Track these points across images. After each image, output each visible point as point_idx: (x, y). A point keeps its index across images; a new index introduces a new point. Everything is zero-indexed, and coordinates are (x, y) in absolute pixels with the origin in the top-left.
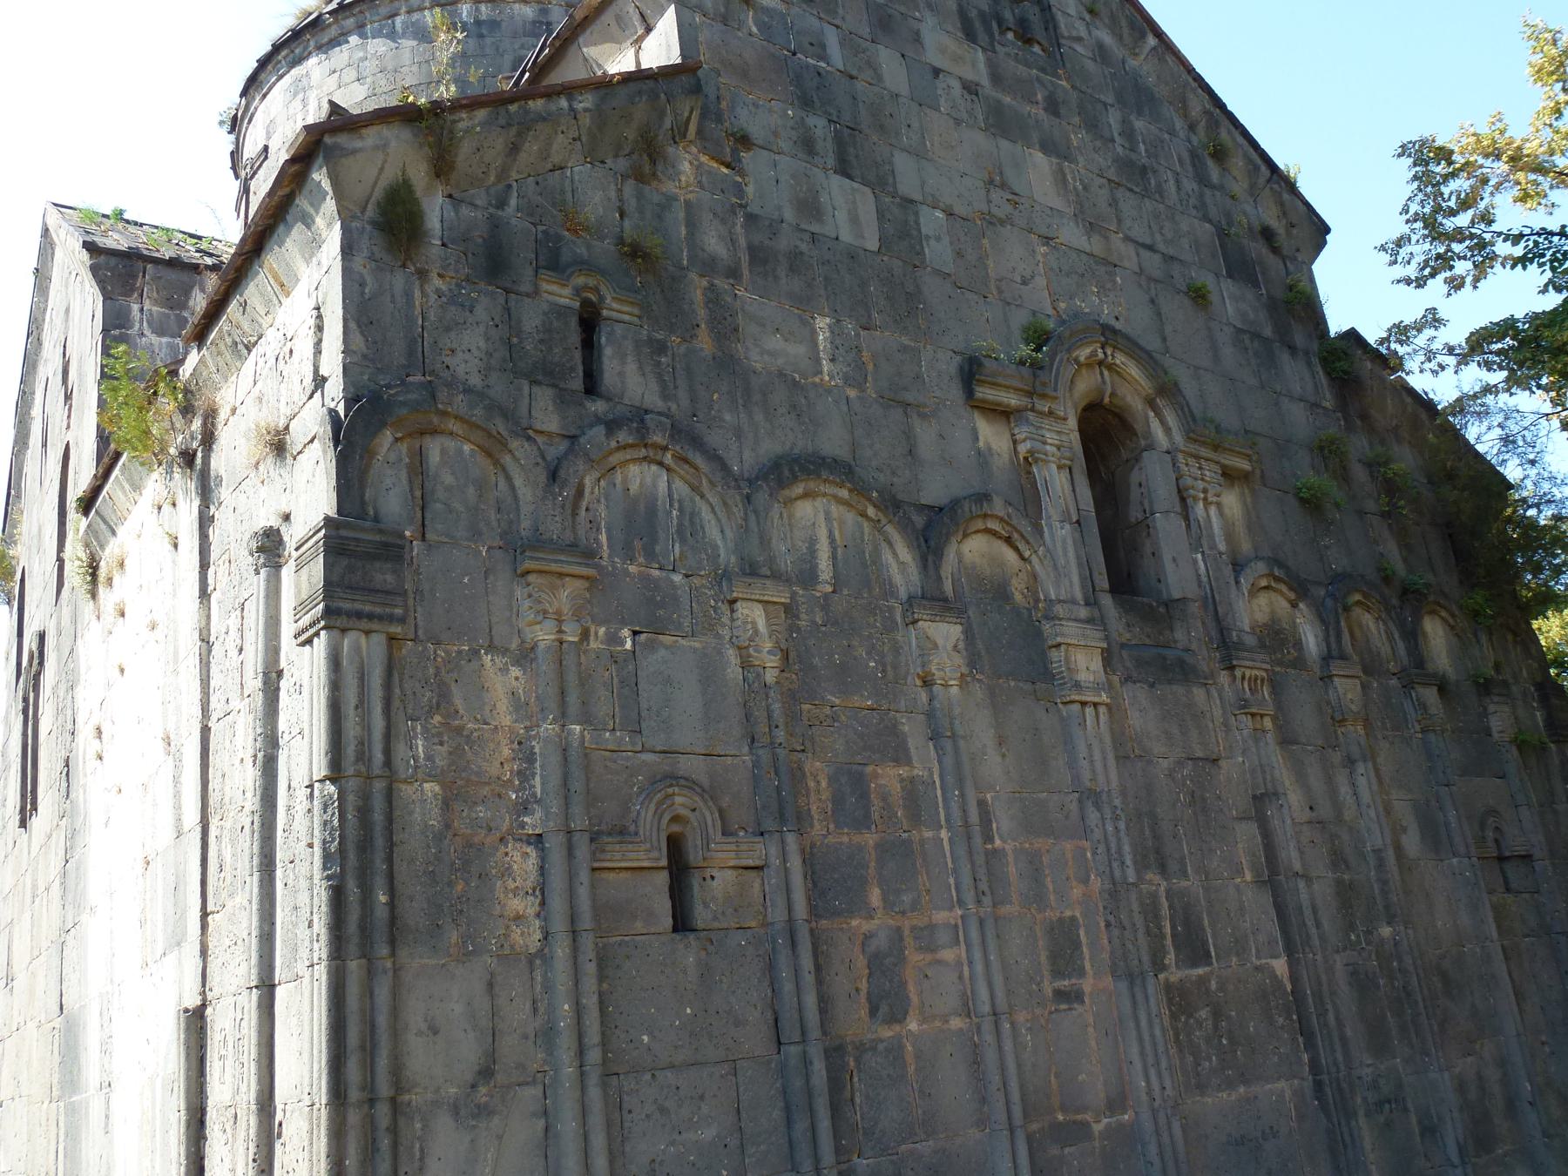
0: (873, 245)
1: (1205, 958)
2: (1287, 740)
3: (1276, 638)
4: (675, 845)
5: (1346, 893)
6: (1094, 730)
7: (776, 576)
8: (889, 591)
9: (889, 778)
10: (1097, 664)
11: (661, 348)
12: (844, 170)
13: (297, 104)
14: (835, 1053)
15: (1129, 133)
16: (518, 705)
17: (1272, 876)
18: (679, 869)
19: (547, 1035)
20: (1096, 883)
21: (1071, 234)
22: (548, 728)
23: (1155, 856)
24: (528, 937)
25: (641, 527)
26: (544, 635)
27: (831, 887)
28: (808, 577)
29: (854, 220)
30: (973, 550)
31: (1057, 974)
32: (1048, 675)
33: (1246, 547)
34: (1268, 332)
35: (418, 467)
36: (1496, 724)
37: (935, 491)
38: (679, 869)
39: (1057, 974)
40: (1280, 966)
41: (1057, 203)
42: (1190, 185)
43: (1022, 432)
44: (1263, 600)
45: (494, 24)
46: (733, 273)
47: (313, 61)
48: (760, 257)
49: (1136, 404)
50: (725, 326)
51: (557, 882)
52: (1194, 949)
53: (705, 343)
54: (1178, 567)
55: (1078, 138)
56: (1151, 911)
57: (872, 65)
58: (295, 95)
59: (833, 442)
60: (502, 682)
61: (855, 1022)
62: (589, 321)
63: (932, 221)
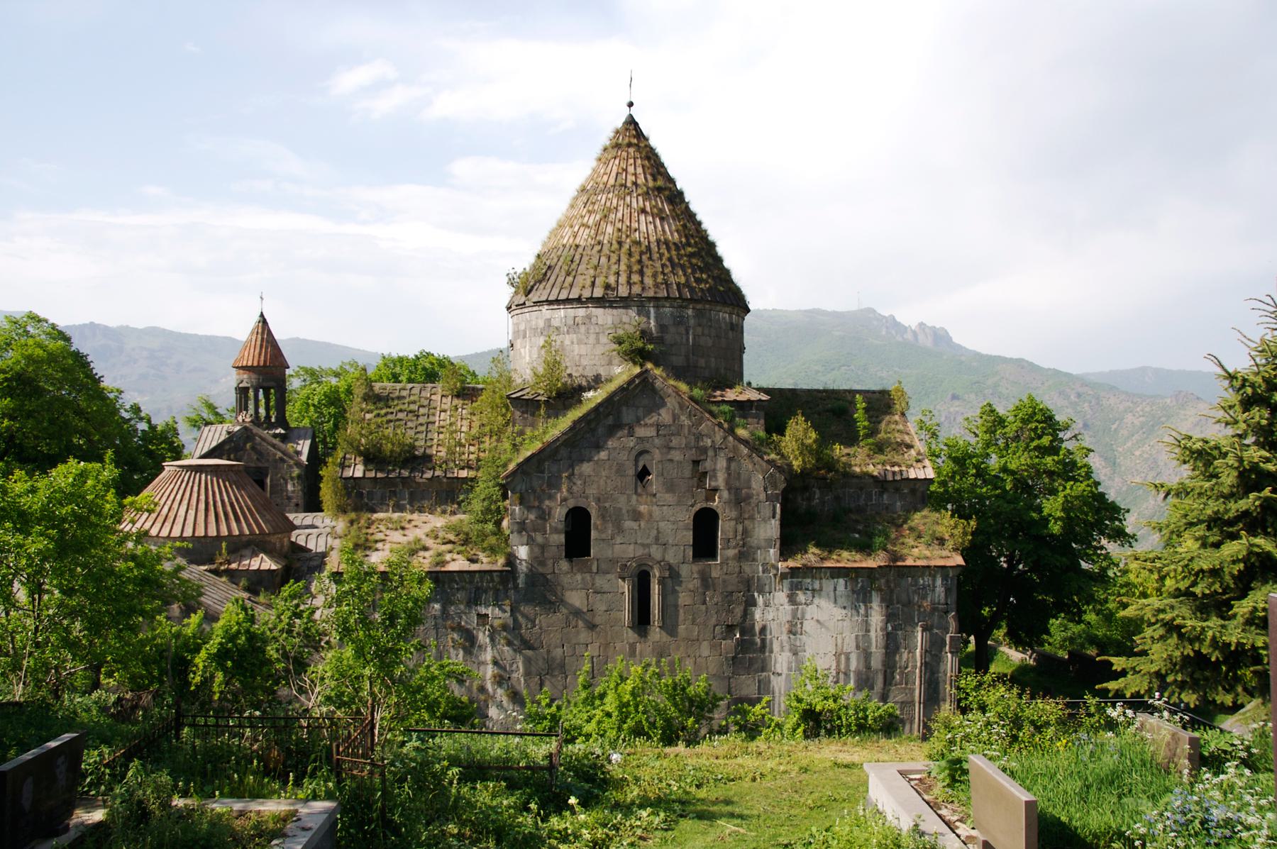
13: (682, 330)
47: (690, 312)
58: (680, 323)
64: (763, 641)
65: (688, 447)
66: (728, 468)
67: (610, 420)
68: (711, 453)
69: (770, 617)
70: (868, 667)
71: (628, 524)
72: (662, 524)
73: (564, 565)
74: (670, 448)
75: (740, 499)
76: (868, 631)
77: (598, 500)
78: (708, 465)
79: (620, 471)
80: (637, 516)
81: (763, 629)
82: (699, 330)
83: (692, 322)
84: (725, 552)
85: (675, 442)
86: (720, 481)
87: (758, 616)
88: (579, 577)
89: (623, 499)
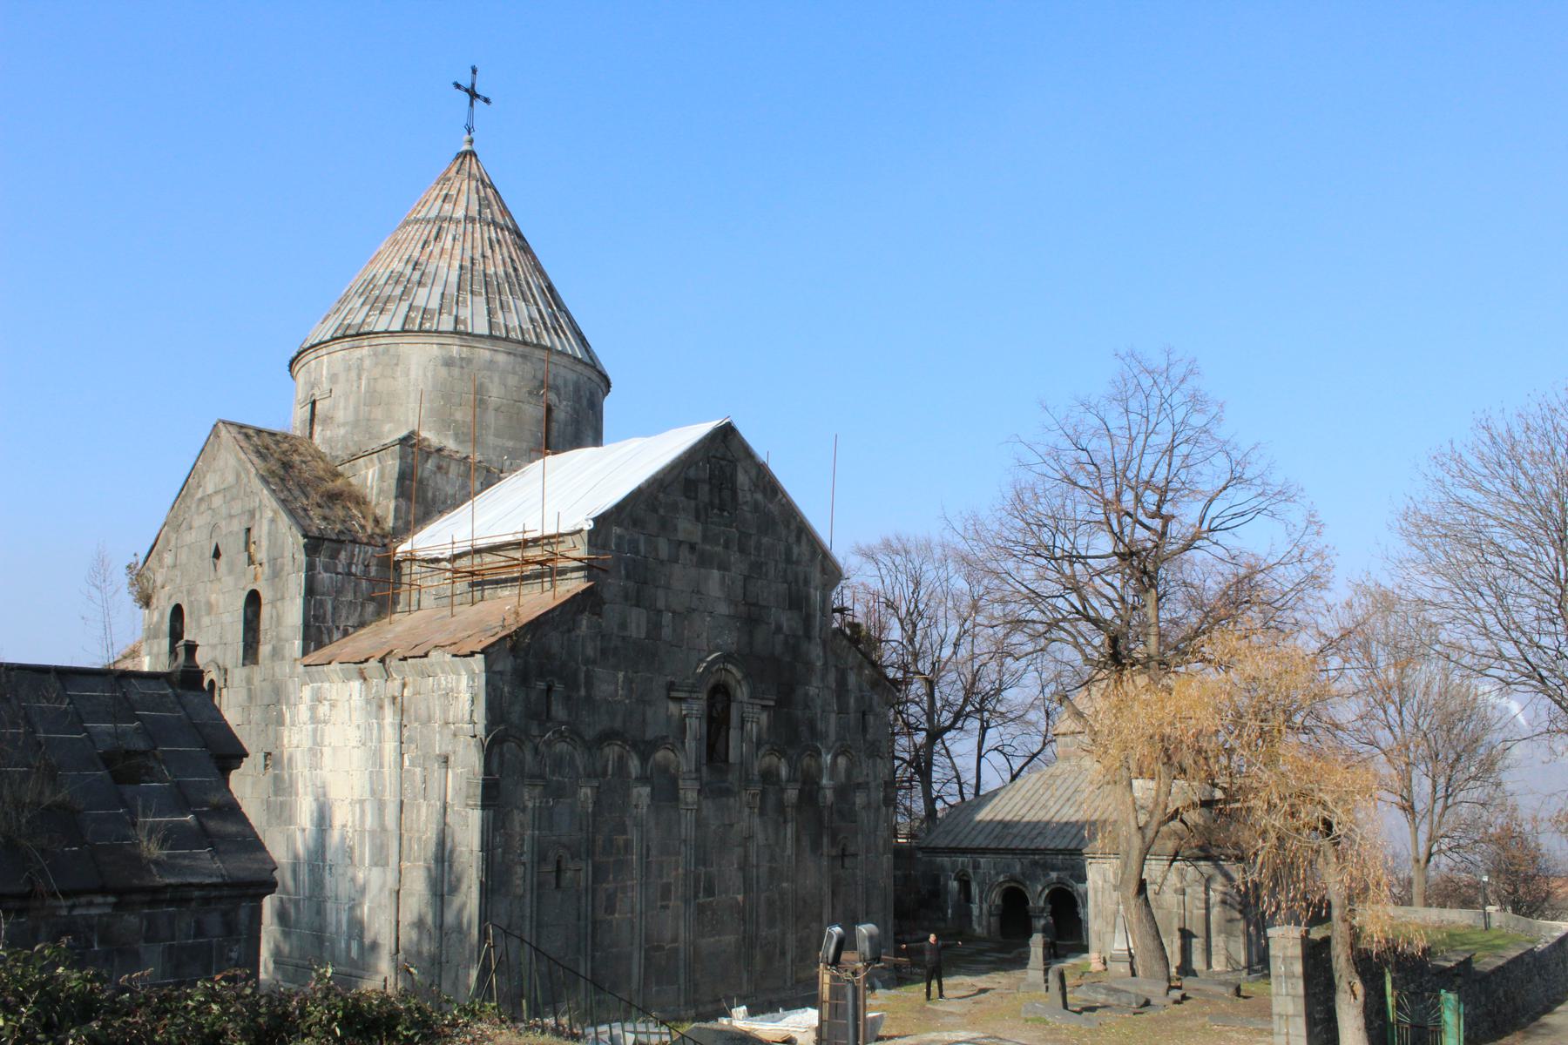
0: (643, 636)
1: (713, 894)
2: (762, 813)
3: (769, 776)
4: (558, 862)
5: (772, 871)
6: (690, 817)
7: (596, 776)
8: (629, 776)
9: (620, 839)
10: (695, 795)
11: (568, 698)
12: (638, 606)
13: (353, 374)
14: (594, 923)
15: (758, 547)
16: (522, 825)
17: (744, 867)
18: (559, 870)
19: (523, 917)
20: (681, 870)
21: (723, 609)
22: (529, 832)
23: (702, 860)
24: (519, 891)
25: (558, 763)
26: (530, 805)
27: (599, 873)
28: (605, 773)
29: (638, 626)
30: (660, 755)
31: (663, 899)
32: (677, 799)
33: (765, 736)
34: (801, 633)
35: (501, 755)
36: (858, 801)
37: (649, 735)
38: (559, 870)
39: (663, 899)
40: (740, 898)
41: (719, 594)
42: (782, 566)
43: (684, 706)
44: (767, 759)
45: (469, 361)
46: (594, 662)
47: (365, 351)
48: (604, 652)
49: (733, 683)
50: (589, 684)
51: (528, 877)
52: (710, 891)
53: (583, 692)
54: (736, 748)
55: (734, 557)
56: (697, 880)
57: (656, 549)
59: (618, 724)
60: (517, 817)
61: (601, 915)
62: (549, 689)
64: (291, 776)
66: (269, 533)
67: (199, 495)
69: (295, 742)
70: (383, 829)
75: (276, 574)
76: (382, 766)
78: (254, 534)
79: (201, 557)
80: (210, 607)
81: (290, 759)
83: (367, 363)
84: (264, 650)
87: (286, 741)
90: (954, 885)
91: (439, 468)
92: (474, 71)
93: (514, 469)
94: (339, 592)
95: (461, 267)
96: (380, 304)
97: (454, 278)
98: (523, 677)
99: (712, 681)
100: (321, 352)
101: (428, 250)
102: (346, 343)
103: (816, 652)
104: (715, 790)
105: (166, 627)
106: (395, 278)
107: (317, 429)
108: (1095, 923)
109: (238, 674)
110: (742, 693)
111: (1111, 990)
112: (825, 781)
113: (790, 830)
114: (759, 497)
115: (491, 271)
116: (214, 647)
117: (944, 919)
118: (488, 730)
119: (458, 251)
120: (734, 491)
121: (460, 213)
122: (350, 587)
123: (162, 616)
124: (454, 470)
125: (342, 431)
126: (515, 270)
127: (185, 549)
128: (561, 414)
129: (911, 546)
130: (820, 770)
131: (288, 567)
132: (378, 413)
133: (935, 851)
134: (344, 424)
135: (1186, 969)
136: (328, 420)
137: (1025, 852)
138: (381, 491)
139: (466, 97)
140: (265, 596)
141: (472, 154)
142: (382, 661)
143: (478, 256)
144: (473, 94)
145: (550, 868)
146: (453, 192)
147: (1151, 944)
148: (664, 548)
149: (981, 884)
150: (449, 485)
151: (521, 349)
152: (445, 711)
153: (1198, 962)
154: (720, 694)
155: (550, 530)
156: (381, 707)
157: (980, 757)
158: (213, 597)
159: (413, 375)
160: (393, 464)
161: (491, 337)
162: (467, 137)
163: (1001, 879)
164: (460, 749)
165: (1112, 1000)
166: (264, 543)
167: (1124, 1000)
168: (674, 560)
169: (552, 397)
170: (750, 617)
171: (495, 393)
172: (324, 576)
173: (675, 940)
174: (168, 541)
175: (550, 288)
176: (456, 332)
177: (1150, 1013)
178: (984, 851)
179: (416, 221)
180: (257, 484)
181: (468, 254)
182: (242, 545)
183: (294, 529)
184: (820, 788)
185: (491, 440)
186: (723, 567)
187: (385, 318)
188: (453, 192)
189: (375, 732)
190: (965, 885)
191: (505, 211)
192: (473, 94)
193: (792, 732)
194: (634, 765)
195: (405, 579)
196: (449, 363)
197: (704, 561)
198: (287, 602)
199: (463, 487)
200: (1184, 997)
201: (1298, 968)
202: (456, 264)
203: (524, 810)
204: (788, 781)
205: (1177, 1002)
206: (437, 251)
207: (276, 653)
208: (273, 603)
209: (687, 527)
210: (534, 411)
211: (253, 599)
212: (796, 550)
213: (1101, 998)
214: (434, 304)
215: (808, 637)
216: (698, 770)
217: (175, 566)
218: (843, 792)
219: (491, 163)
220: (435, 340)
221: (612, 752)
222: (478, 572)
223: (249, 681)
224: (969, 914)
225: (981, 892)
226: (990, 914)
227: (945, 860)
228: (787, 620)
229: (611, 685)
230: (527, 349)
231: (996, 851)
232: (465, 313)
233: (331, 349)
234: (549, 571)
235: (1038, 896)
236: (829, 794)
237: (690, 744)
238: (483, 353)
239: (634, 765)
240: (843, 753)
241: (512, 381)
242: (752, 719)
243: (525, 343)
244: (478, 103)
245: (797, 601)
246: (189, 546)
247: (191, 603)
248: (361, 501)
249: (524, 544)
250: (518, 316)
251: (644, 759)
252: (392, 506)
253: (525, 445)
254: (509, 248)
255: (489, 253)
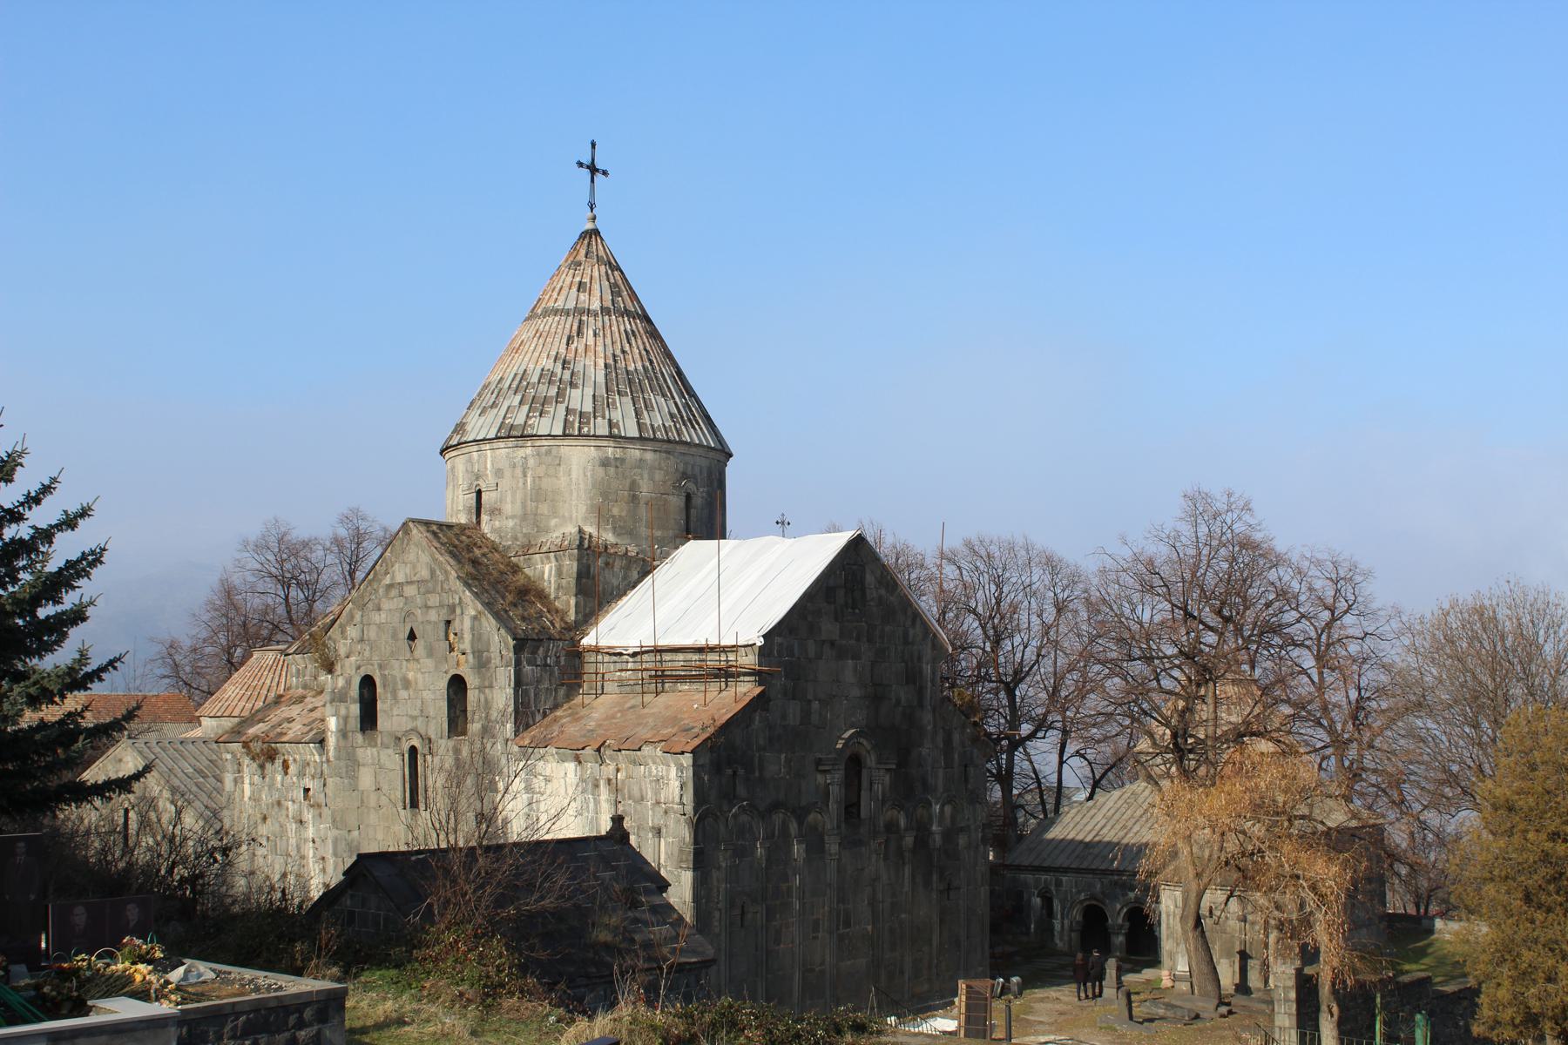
2: (886, 859)
3: (891, 827)
9: (784, 886)
13: (519, 471)
18: (743, 913)
21: (856, 692)
30: (811, 817)
37: (803, 803)
38: (743, 913)
40: (869, 928)
45: (622, 460)
47: (529, 451)
49: (864, 753)
52: (847, 924)
54: (866, 807)
60: (715, 874)
62: (735, 773)
63: (816, 705)
65: (442, 606)
66: (472, 629)
67: (387, 580)
68: (458, 611)
71: (403, 694)
72: (425, 693)
73: (359, 737)
74: (428, 607)
75: (482, 664)
77: (380, 667)
78: (456, 625)
79: (395, 636)
80: (407, 684)
82: (541, 471)
83: (531, 462)
84: (474, 727)
85: (434, 600)
86: (466, 645)
88: (369, 751)
89: (396, 664)
90: (1037, 901)
91: (607, 564)
92: (593, 145)
93: (665, 556)
94: (539, 681)
95: (606, 366)
96: (539, 406)
97: (601, 379)
98: (717, 768)
99: (848, 753)
100: (483, 447)
101: (573, 347)
102: (511, 442)
103: (927, 718)
104: (851, 843)
105: (355, 691)
106: (547, 377)
107: (485, 518)
108: (1166, 945)
109: (444, 745)
110: (871, 760)
111: (1169, 1006)
112: (934, 828)
113: (907, 871)
114: (883, 592)
115: (631, 368)
116: (414, 718)
117: (1028, 933)
118: (696, 810)
119: (600, 349)
120: (863, 591)
121: (596, 305)
122: (546, 676)
123: (349, 682)
124: (618, 564)
125: (511, 523)
126: (651, 362)
127: (373, 628)
128: (698, 501)
129: (994, 549)
130: (930, 818)
131: (496, 660)
132: (544, 509)
133: (1019, 868)
134: (513, 517)
135: (1243, 988)
136: (495, 512)
137: (1105, 872)
138: (559, 587)
139: (586, 173)
140: (472, 681)
141: (596, 232)
142: (598, 750)
143: (618, 352)
144: (593, 169)
145: (738, 912)
146: (586, 280)
147: (1205, 969)
148: (812, 648)
149: (1063, 902)
150: (614, 579)
151: (665, 446)
152: (657, 793)
153: (1254, 980)
154: (854, 764)
155: (727, 641)
156: (597, 786)
157: (1061, 763)
158: (411, 675)
159: (574, 476)
160: (571, 566)
161: (641, 439)
162: (590, 214)
163: (1082, 897)
164: (671, 823)
165: (1169, 1014)
166: (467, 637)
167: (1179, 1013)
168: (819, 657)
169: (692, 486)
170: (876, 696)
171: (645, 489)
172: (528, 669)
173: (822, 963)
174: (352, 617)
175: (680, 373)
176: (611, 436)
177: (1199, 1024)
178: (1066, 870)
179: (556, 312)
180: (459, 586)
181: (609, 354)
182: (442, 634)
183: (503, 631)
184: (931, 833)
185: (644, 531)
186: (856, 657)
187: (546, 421)
188: (586, 280)
189: (591, 805)
190: (1048, 901)
191: (633, 296)
192: (593, 169)
193: (908, 790)
194: (793, 827)
195: (589, 668)
196: (605, 463)
197: (842, 654)
198: (496, 691)
199: (625, 578)
200: (1230, 1012)
201: (1293, 995)
202: (601, 363)
203: (719, 868)
204: (906, 830)
205: (1223, 1016)
206: (581, 349)
207: (486, 731)
208: (481, 689)
209: (829, 628)
210: (676, 502)
211: (457, 685)
212: (911, 632)
213: (1161, 1012)
214: (588, 407)
215: (921, 706)
216: (839, 827)
217: (362, 640)
218: (949, 835)
219: (616, 242)
220: (593, 443)
221: (778, 818)
222: (661, 668)
223: (457, 751)
224: (1052, 929)
225: (1063, 909)
226: (1071, 930)
227: (1029, 877)
228: (903, 693)
229: (776, 765)
230: (670, 446)
231: (1078, 871)
232: (616, 416)
233: (495, 445)
234: (725, 674)
235: (1117, 915)
236: (938, 838)
237: (832, 806)
238: (635, 453)
239: (793, 827)
240: (949, 802)
241: (658, 476)
242: (878, 780)
243: (669, 441)
244: (599, 177)
245: (912, 677)
246: (379, 626)
247: (384, 677)
248: (542, 596)
249: (700, 650)
250: (660, 415)
251: (800, 824)
252: (573, 601)
253: (671, 533)
254: (642, 341)
255: (627, 348)
